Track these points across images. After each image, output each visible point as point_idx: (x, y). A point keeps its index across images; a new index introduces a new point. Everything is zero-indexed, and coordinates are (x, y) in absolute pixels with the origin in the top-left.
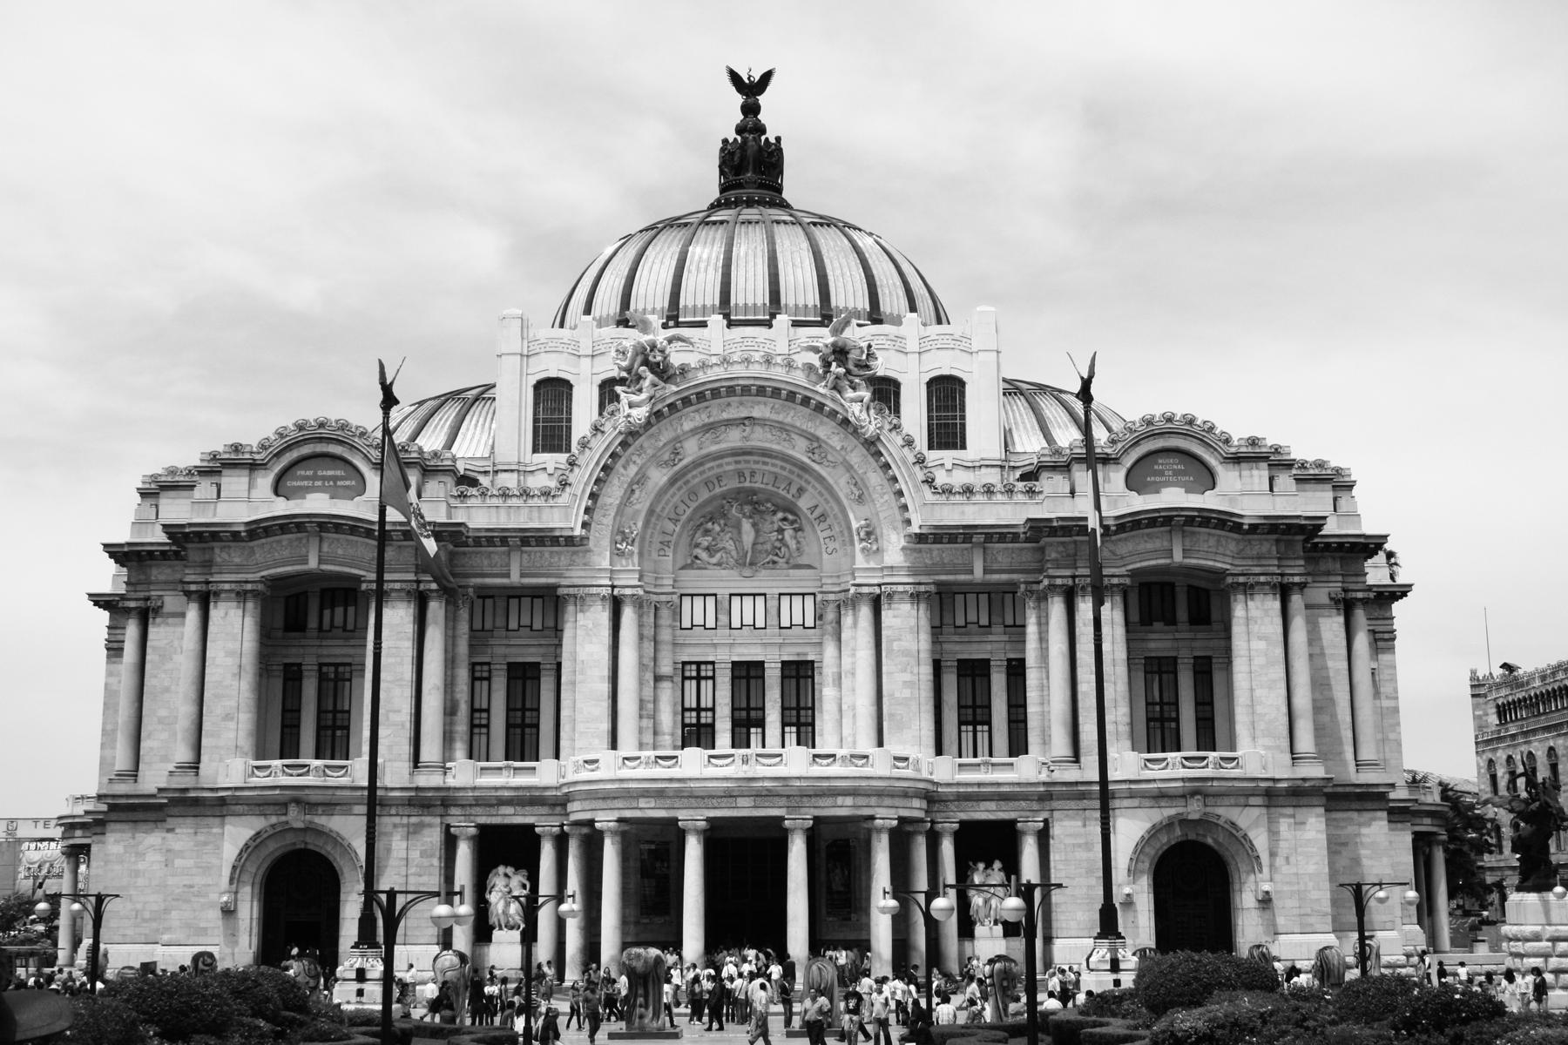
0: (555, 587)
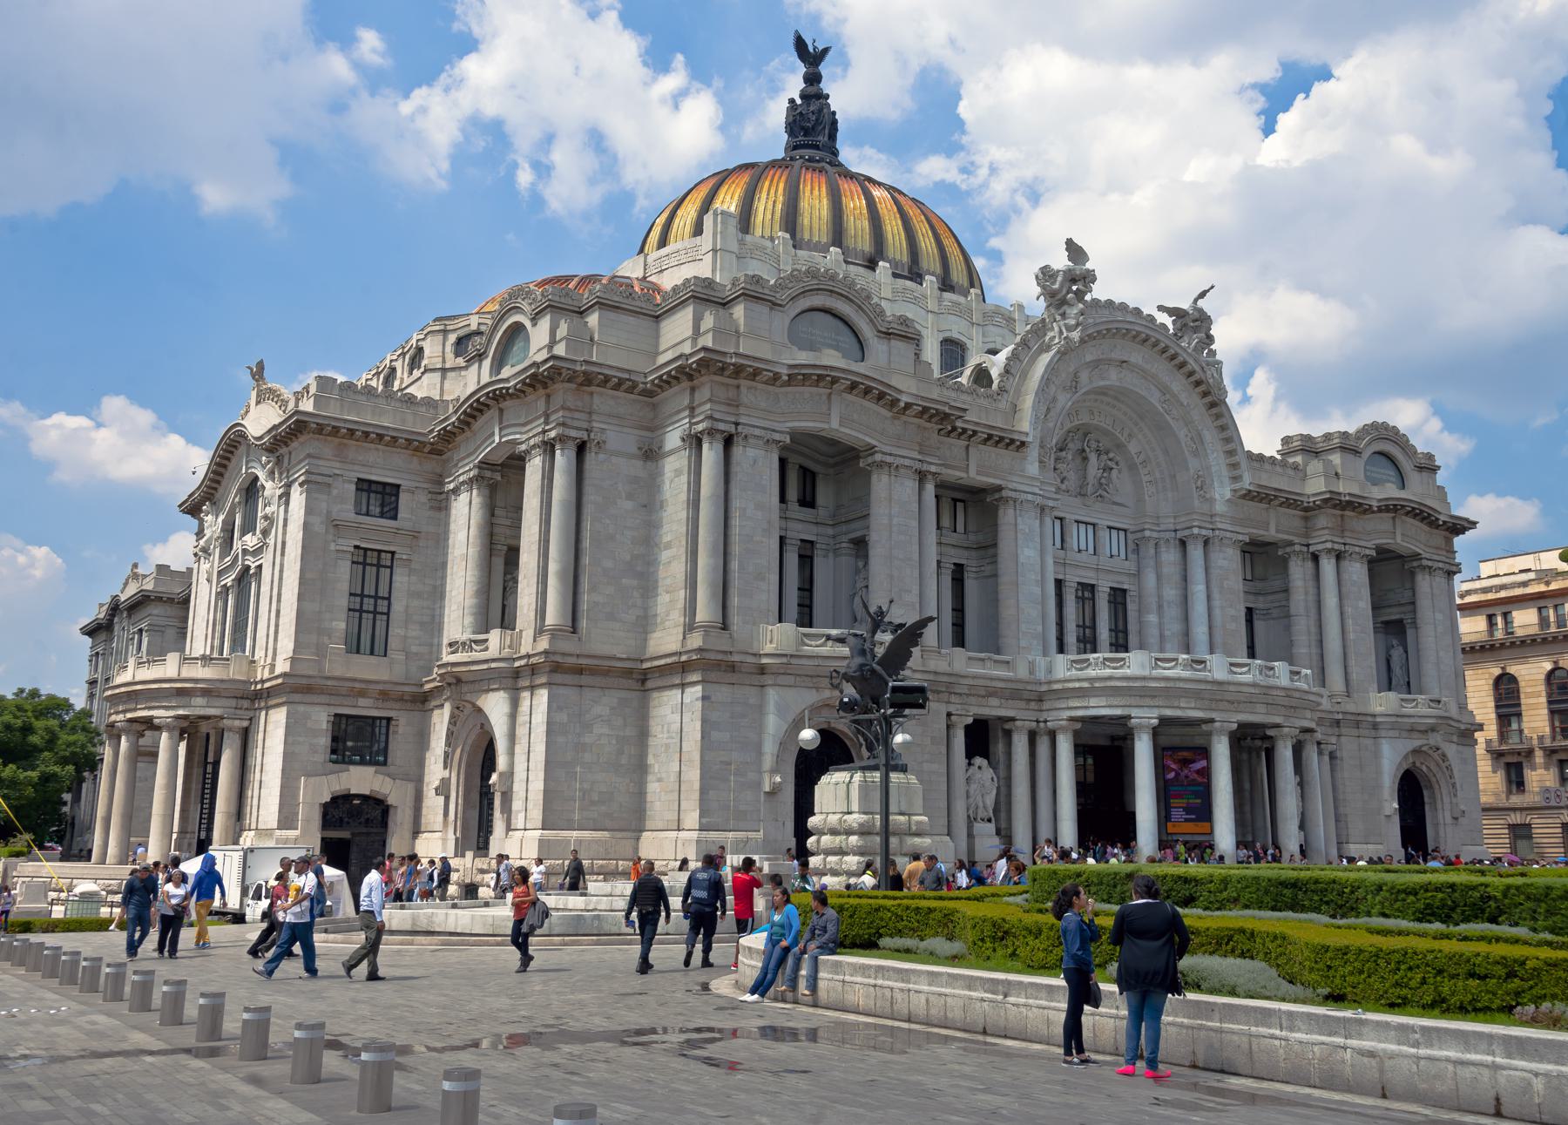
0: (999, 489)
